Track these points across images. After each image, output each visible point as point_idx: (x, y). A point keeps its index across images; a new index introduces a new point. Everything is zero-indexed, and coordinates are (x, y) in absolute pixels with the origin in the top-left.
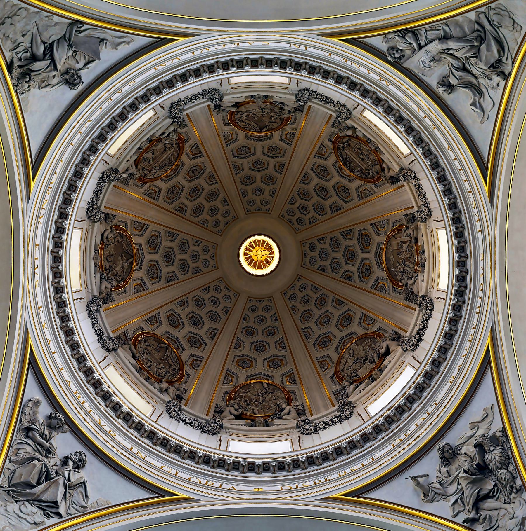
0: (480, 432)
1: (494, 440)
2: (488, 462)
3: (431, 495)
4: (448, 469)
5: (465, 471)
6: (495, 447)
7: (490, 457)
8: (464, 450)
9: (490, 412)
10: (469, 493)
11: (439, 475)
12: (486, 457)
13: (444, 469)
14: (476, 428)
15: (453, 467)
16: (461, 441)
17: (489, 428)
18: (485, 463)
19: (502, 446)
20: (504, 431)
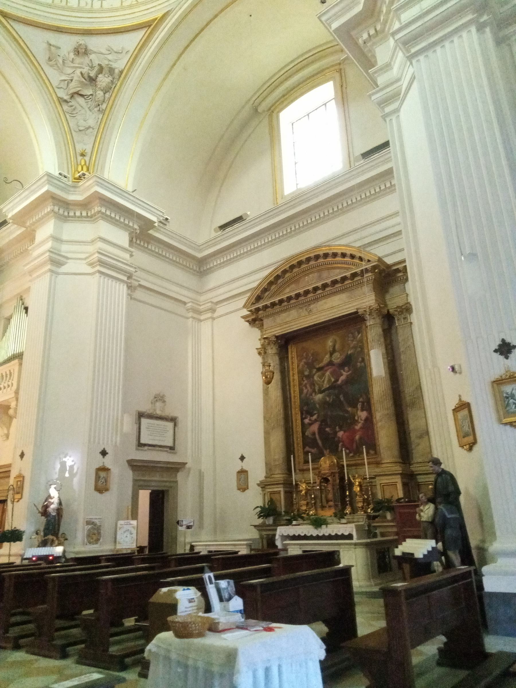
0: (110, 57)
1: (111, 71)
2: (98, 79)
3: (52, 63)
4: (74, 58)
5: (82, 73)
6: (109, 76)
7: (101, 79)
8: (92, 56)
9: (124, 52)
10: (74, 87)
11: (67, 55)
12: (100, 76)
13: (72, 56)
14: (109, 52)
15: (78, 60)
16: (95, 50)
17: (116, 61)
18: (96, 78)
19: (114, 78)
20: (121, 72)
